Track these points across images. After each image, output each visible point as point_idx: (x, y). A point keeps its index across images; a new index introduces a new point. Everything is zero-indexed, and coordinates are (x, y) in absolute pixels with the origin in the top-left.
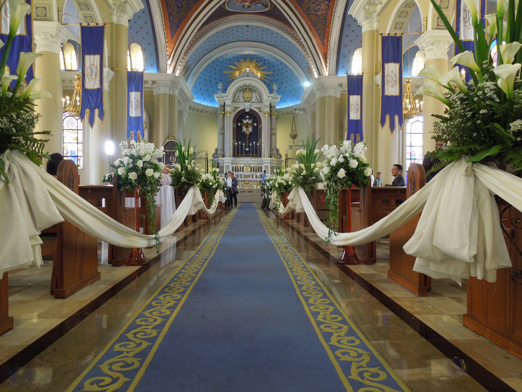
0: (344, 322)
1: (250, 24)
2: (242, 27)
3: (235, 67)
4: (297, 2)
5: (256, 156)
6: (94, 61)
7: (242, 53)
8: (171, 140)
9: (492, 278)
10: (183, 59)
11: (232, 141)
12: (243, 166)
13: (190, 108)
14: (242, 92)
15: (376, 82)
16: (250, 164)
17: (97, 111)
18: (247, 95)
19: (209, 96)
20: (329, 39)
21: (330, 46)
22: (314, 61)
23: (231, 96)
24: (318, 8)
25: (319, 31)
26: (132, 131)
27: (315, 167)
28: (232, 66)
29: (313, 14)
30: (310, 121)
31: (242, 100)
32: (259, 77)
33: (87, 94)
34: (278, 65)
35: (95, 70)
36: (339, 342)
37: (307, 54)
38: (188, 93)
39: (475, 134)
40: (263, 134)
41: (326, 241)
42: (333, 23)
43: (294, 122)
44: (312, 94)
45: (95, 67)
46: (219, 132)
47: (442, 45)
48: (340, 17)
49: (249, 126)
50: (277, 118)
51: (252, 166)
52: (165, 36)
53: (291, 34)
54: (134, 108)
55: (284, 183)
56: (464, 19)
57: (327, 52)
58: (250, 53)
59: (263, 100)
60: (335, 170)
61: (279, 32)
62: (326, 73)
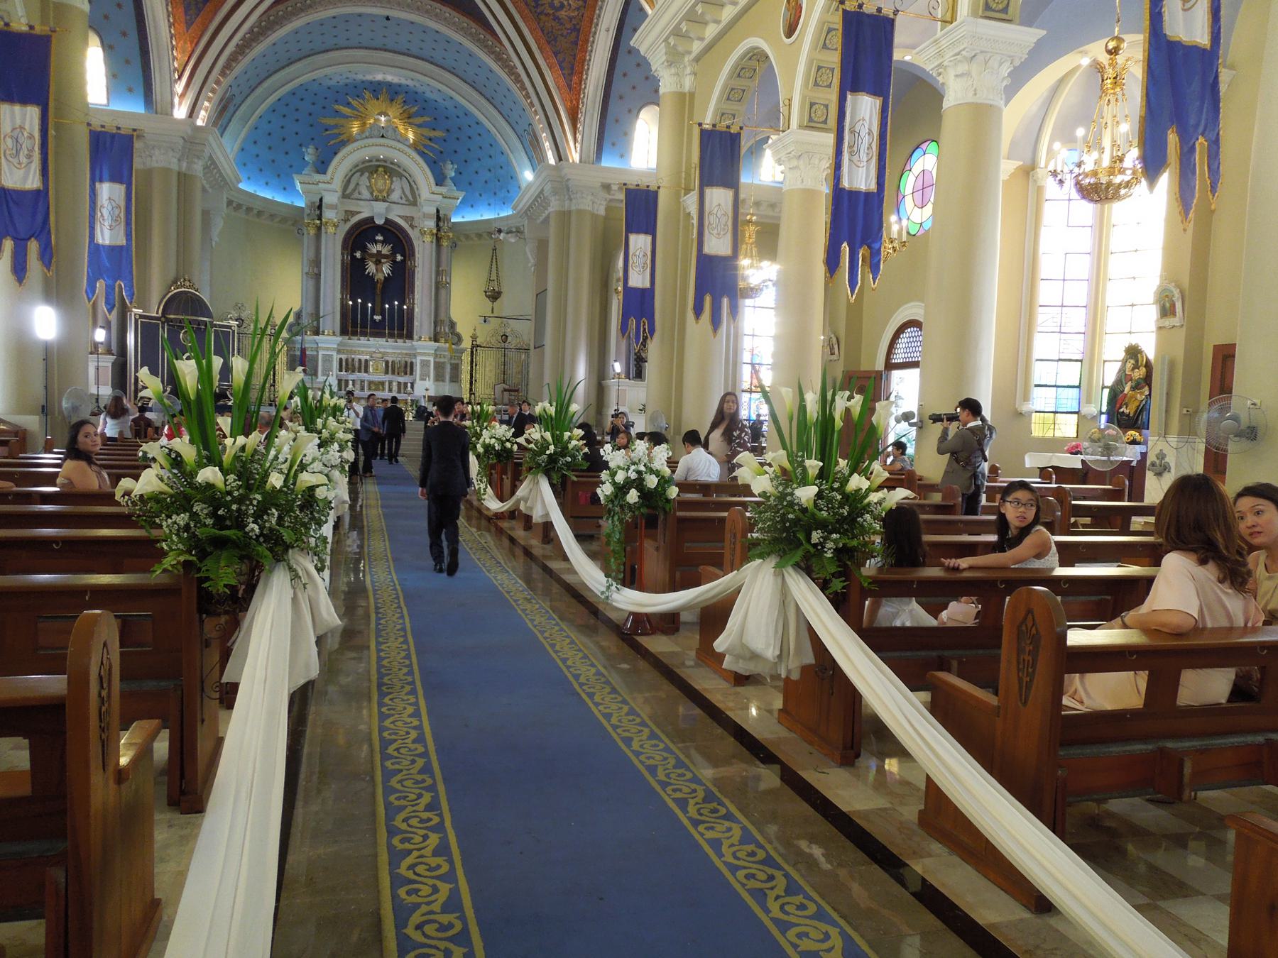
0: (643, 724)
1: (393, 13)
2: (373, 19)
3: (349, 110)
5: (400, 336)
6: (24, 119)
7: (369, 78)
8: (183, 289)
9: (795, 676)
10: (218, 82)
11: (339, 296)
12: (368, 357)
13: (230, 203)
14: (367, 174)
15: (684, 209)
16: (384, 354)
17: (33, 247)
18: (380, 183)
19: (279, 176)
20: (584, 77)
21: (584, 93)
22: (547, 125)
23: (337, 184)
25: (560, 56)
26: (101, 280)
27: (570, 438)
28: (341, 107)
29: (547, 15)
31: (366, 194)
32: (411, 141)
33: (7, 202)
34: (458, 117)
35: (26, 144)
36: (641, 746)
37: (532, 105)
38: (226, 166)
39: (784, 535)
40: (417, 283)
41: (603, 597)
42: (593, 42)
43: (494, 260)
44: (540, 199)
45: (26, 134)
46: (306, 270)
47: (817, 162)
49: (383, 260)
50: (454, 245)
51: (390, 359)
52: (169, 21)
53: (493, 53)
54: (106, 224)
55: (496, 445)
56: (851, 147)
57: (578, 107)
58: (389, 78)
59: (418, 200)
60: (621, 490)
61: (467, 43)
62: (574, 156)
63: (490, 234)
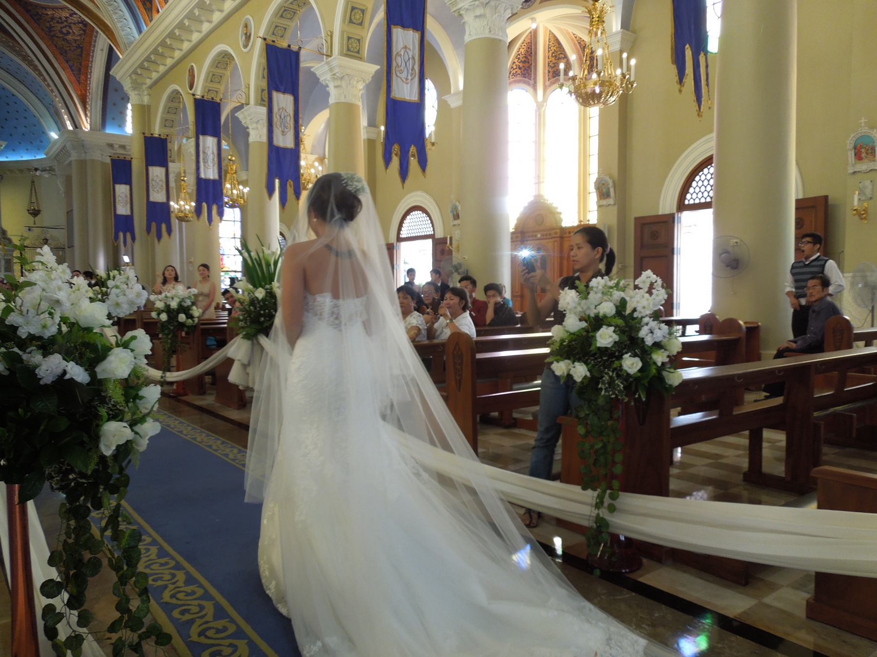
4: (31, 16)
20: (89, 76)
22: (64, 104)
24: (68, 31)
25: (70, 63)
30: (62, 190)
48: (105, 51)
56: (204, 159)
62: (86, 126)
63: (29, 170)
